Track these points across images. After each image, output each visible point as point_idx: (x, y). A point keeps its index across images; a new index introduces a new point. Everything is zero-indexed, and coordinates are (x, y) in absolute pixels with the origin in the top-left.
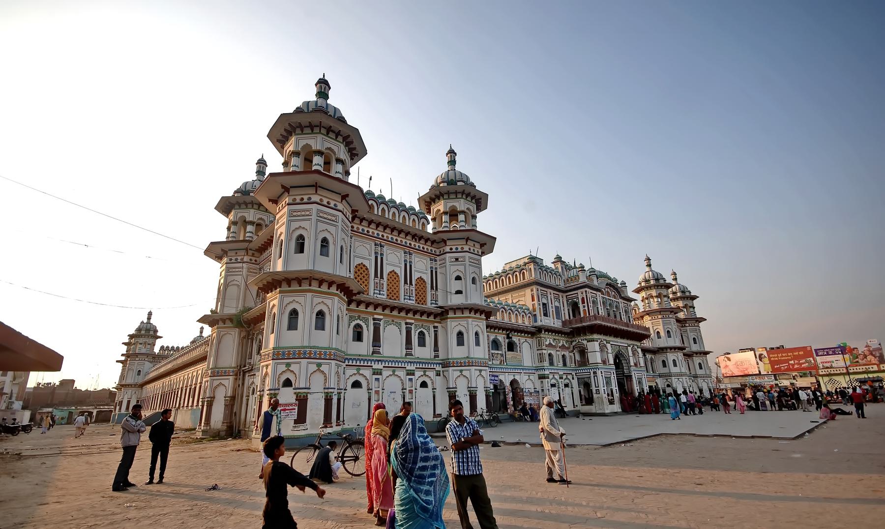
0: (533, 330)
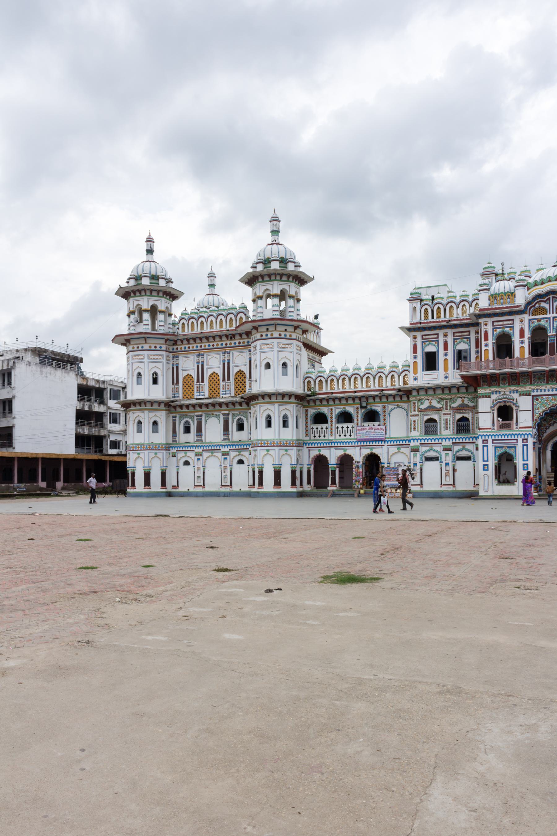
0: (400, 393)
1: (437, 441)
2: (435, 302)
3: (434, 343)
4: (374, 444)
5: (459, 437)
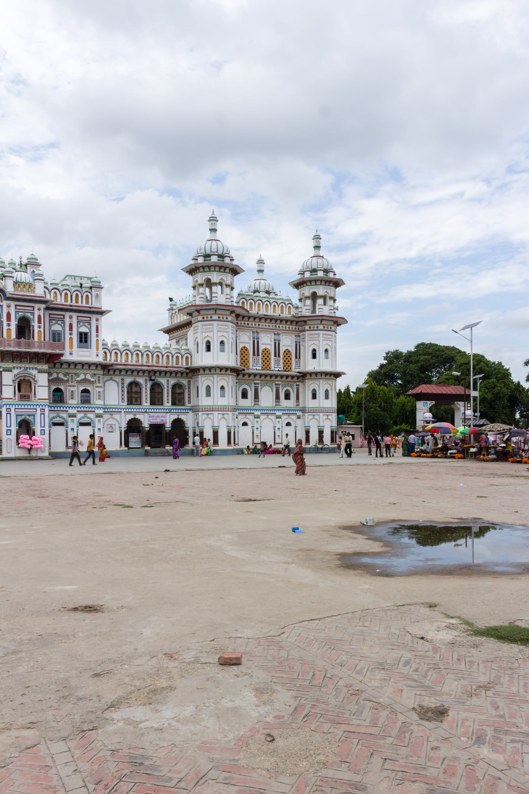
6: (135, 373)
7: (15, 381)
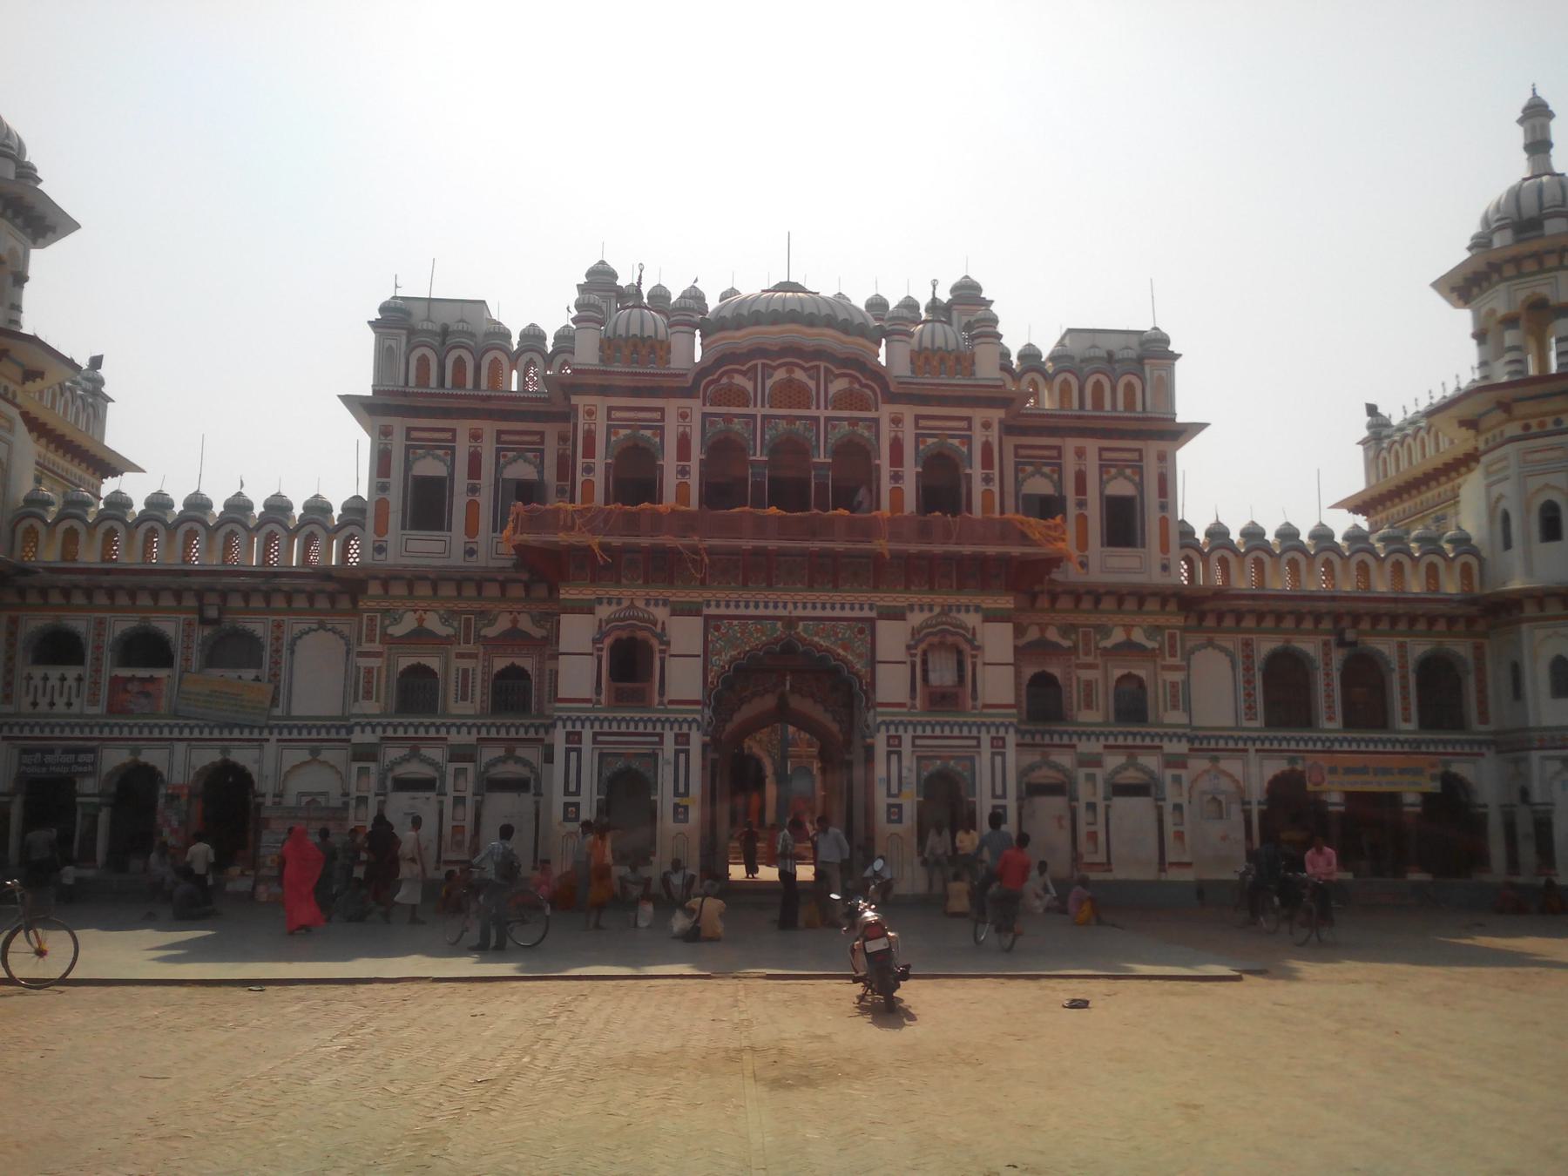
0: (330, 586)
1: (432, 733)
2: (450, 341)
3: (441, 452)
4: (236, 734)
5: (499, 722)
6: (1289, 623)
7: (915, 647)
